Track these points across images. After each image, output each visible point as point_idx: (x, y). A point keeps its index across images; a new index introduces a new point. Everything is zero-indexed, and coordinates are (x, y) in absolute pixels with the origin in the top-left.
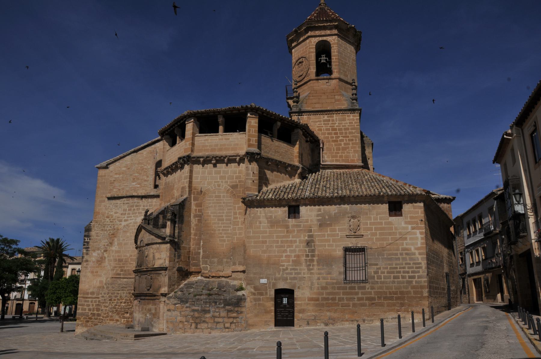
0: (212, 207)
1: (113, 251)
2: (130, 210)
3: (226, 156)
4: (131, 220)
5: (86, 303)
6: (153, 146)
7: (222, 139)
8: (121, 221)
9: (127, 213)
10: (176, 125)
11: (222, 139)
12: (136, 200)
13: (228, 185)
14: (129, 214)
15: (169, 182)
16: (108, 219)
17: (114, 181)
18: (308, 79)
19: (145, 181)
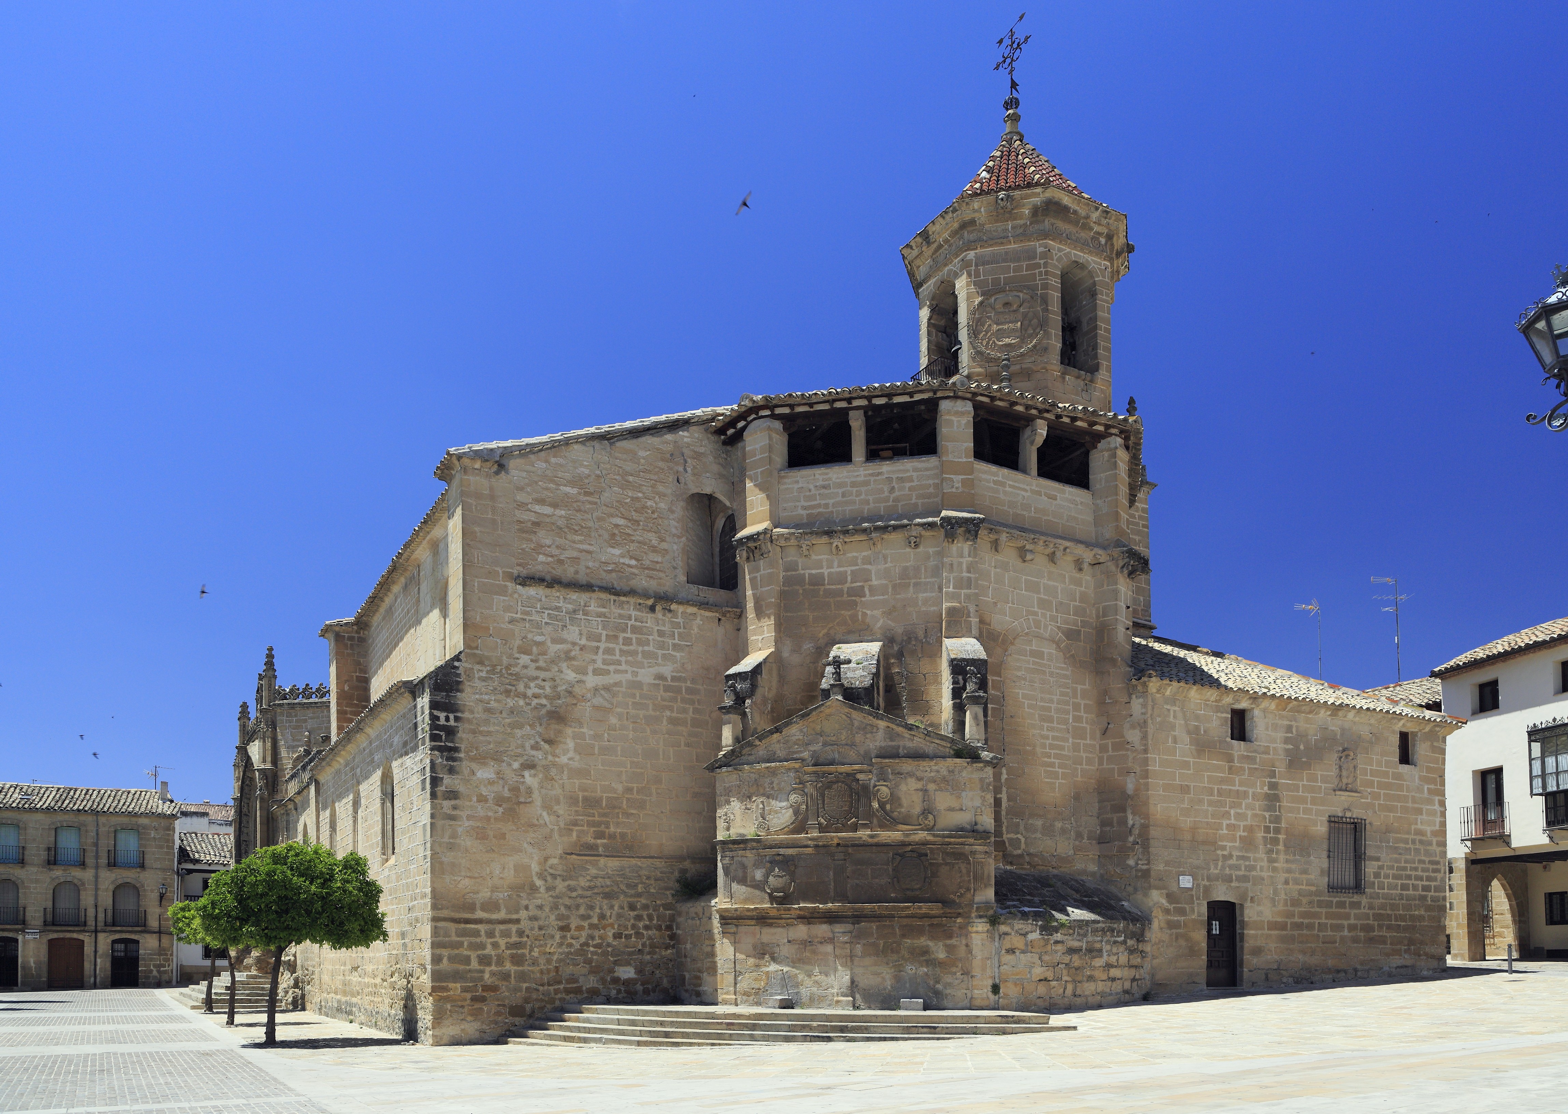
0: (1025, 679)
1: (561, 768)
2: (612, 638)
4: (617, 672)
5: (466, 941)
6: (669, 437)
7: (1039, 493)
8: (582, 671)
9: (602, 645)
12: (630, 609)
14: (608, 651)
15: (817, 581)
16: (525, 659)
17: (537, 524)
19: (654, 549)
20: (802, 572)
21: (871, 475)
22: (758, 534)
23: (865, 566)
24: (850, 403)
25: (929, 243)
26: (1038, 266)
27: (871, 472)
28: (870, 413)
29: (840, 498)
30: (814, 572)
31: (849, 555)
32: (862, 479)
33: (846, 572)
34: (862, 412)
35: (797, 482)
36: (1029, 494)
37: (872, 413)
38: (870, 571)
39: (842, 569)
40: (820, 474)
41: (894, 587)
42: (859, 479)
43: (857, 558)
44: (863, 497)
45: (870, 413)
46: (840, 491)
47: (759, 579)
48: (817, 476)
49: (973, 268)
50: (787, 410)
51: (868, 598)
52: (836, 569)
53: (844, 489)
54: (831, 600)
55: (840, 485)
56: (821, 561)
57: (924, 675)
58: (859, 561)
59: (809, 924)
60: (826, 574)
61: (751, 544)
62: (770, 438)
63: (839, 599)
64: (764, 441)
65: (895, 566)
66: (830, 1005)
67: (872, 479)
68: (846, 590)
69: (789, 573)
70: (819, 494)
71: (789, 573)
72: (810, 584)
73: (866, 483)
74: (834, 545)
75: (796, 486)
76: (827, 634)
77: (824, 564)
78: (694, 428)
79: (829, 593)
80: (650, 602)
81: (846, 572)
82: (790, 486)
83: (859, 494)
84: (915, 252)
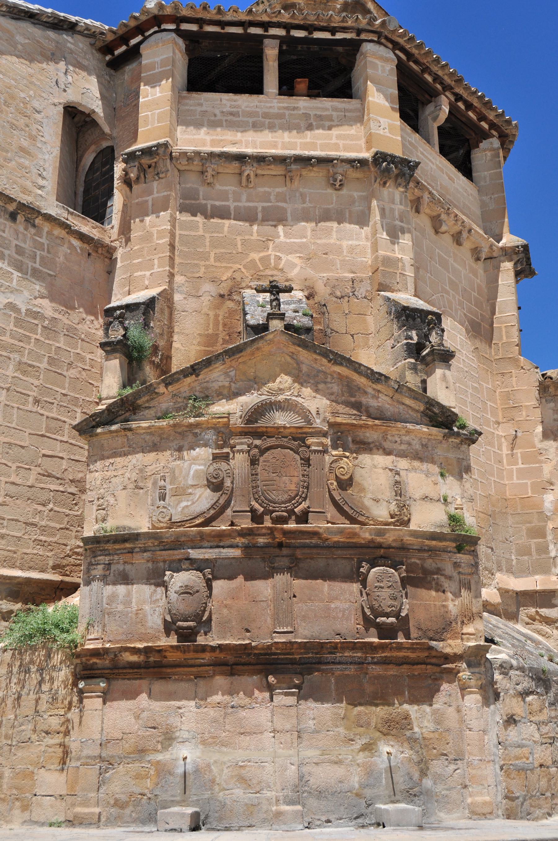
6: (51, 34)
10: (281, 32)
13: (465, 315)
19: (22, 149)
20: (204, 202)
21: (287, 108)
22: (158, 146)
23: (280, 204)
24: (266, 30)
27: (286, 105)
28: (284, 48)
30: (217, 203)
31: (261, 190)
32: (276, 111)
34: (277, 42)
35: (201, 105)
37: (288, 45)
38: (285, 210)
39: (251, 204)
40: (228, 100)
42: (272, 111)
43: (269, 194)
45: (284, 48)
46: (251, 120)
47: (150, 203)
48: (224, 102)
50: (194, 27)
51: (282, 239)
53: (255, 119)
55: (251, 114)
56: (226, 192)
57: (352, 336)
58: (272, 197)
59: (232, 674)
60: (232, 208)
61: (145, 161)
62: (174, 53)
63: (247, 237)
64: (164, 53)
65: (315, 207)
66: (264, 821)
67: (287, 112)
69: (187, 202)
70: (226, 121)
71: (187, 202)
74: (246, 174)
75: (199, 109)
77: (230, 196)
78: (79, 37)
80: (11, 207)
82: (192, 108)
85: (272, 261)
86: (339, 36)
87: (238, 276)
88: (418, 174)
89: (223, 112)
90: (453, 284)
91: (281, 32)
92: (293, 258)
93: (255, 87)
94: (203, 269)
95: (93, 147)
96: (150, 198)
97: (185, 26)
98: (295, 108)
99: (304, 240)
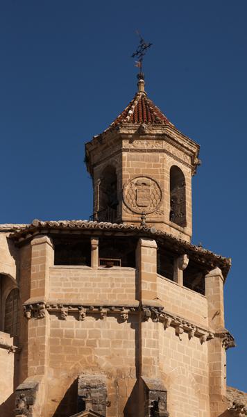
3: (196, 327)
11: (183, 295)
15: (69, 335)
18: (160, 220)
20: (61, 328)
21: (102, 275)
25: (102, 144)
26: (159, 166)
29: (83, 287)
30: (68, 329)
33: (86, 331)
35: (60, 274)
36: (179, 295)
38: (99, 331)
41: (113, 342)
44: (97, 287)
46: (84, 283)
49: (126, 161)
50: (57, 232)
51: (98, 347)
52: (80, 328)
54: (78, 347)
55: (85, 279)
58: (94, 325)
64: (44, 250)
68: (85, 342)
72: (66, 336)
73: (99, 280)
75: (59, 277)
76: (75, 368)
79: (76, 343)
81: (86, 331)
83: (94, 285)
84: (94, 147)
85: (93, 359)
86: (127, 235)
87: (77, 367)
88: (164, 311)
89: (71, 278)
90: (186, 359)
91: (100, 233)
92: (103, 358)
93: (88, 263)
94: (61, 364)
95: (9, 288)
96: (36, 327)
97: (52, 232)
98: (106, 275)
99: (108, 348)
